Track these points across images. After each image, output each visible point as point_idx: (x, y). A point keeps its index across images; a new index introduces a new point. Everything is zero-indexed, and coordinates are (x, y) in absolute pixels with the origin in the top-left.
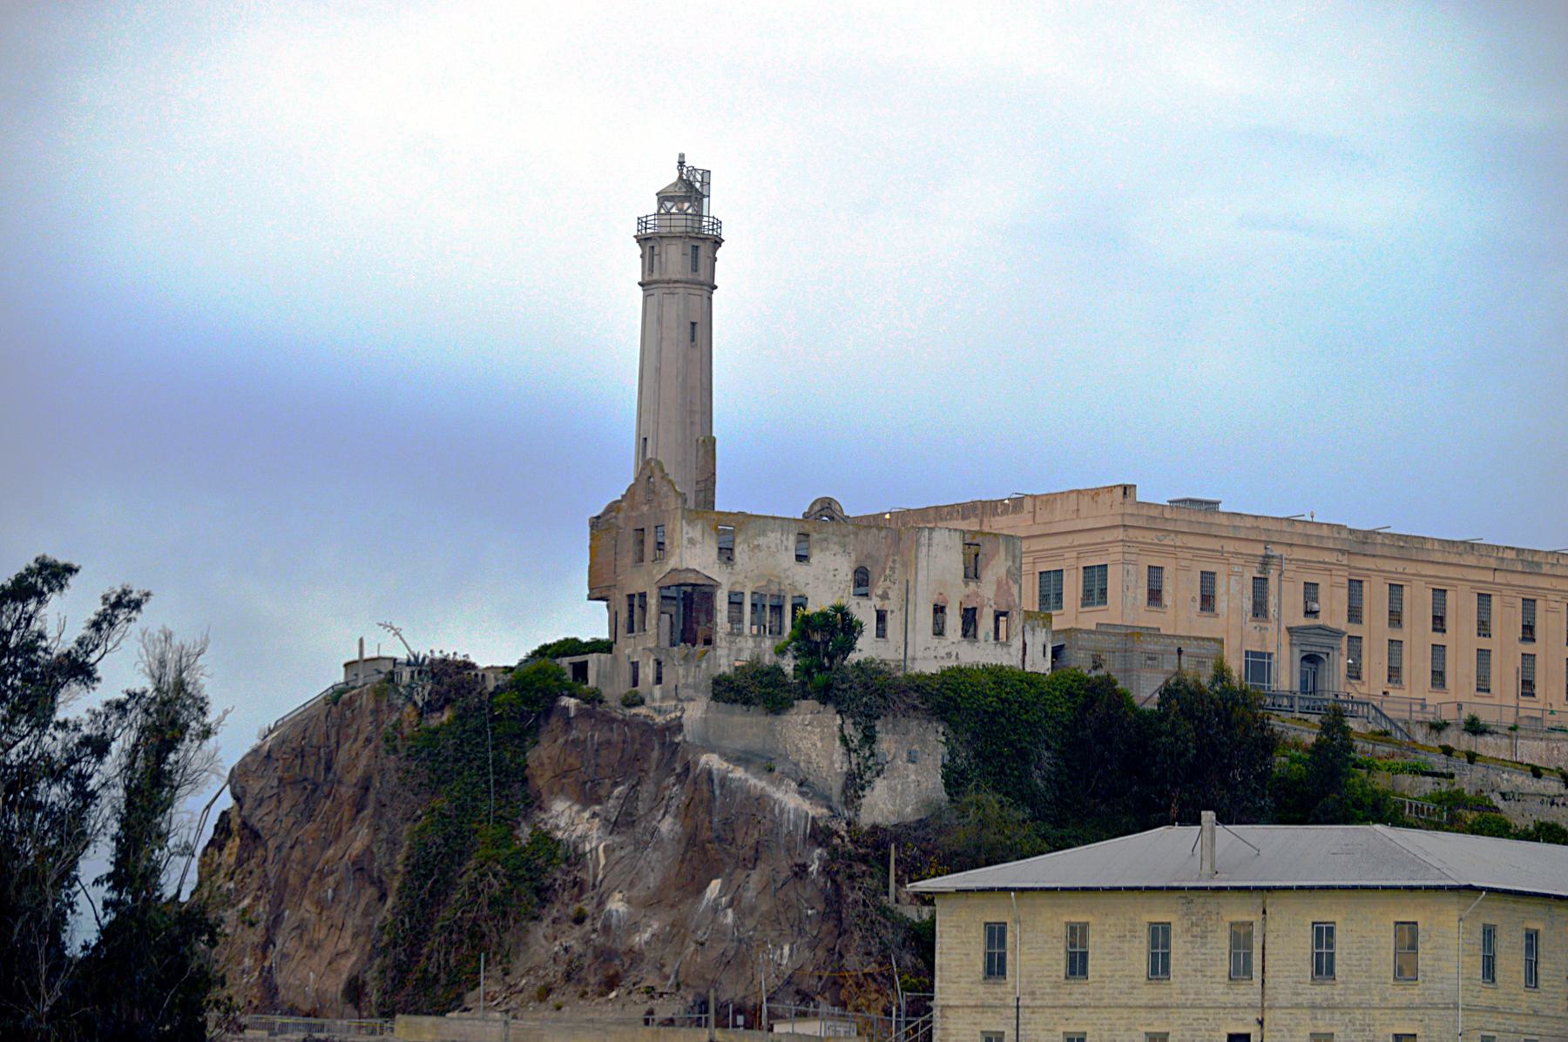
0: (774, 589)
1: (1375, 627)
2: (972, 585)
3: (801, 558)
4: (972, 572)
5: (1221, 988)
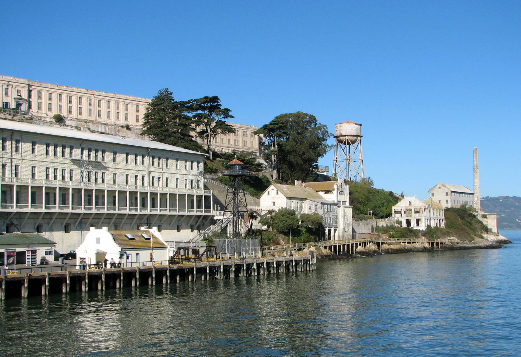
1: (34, 100)
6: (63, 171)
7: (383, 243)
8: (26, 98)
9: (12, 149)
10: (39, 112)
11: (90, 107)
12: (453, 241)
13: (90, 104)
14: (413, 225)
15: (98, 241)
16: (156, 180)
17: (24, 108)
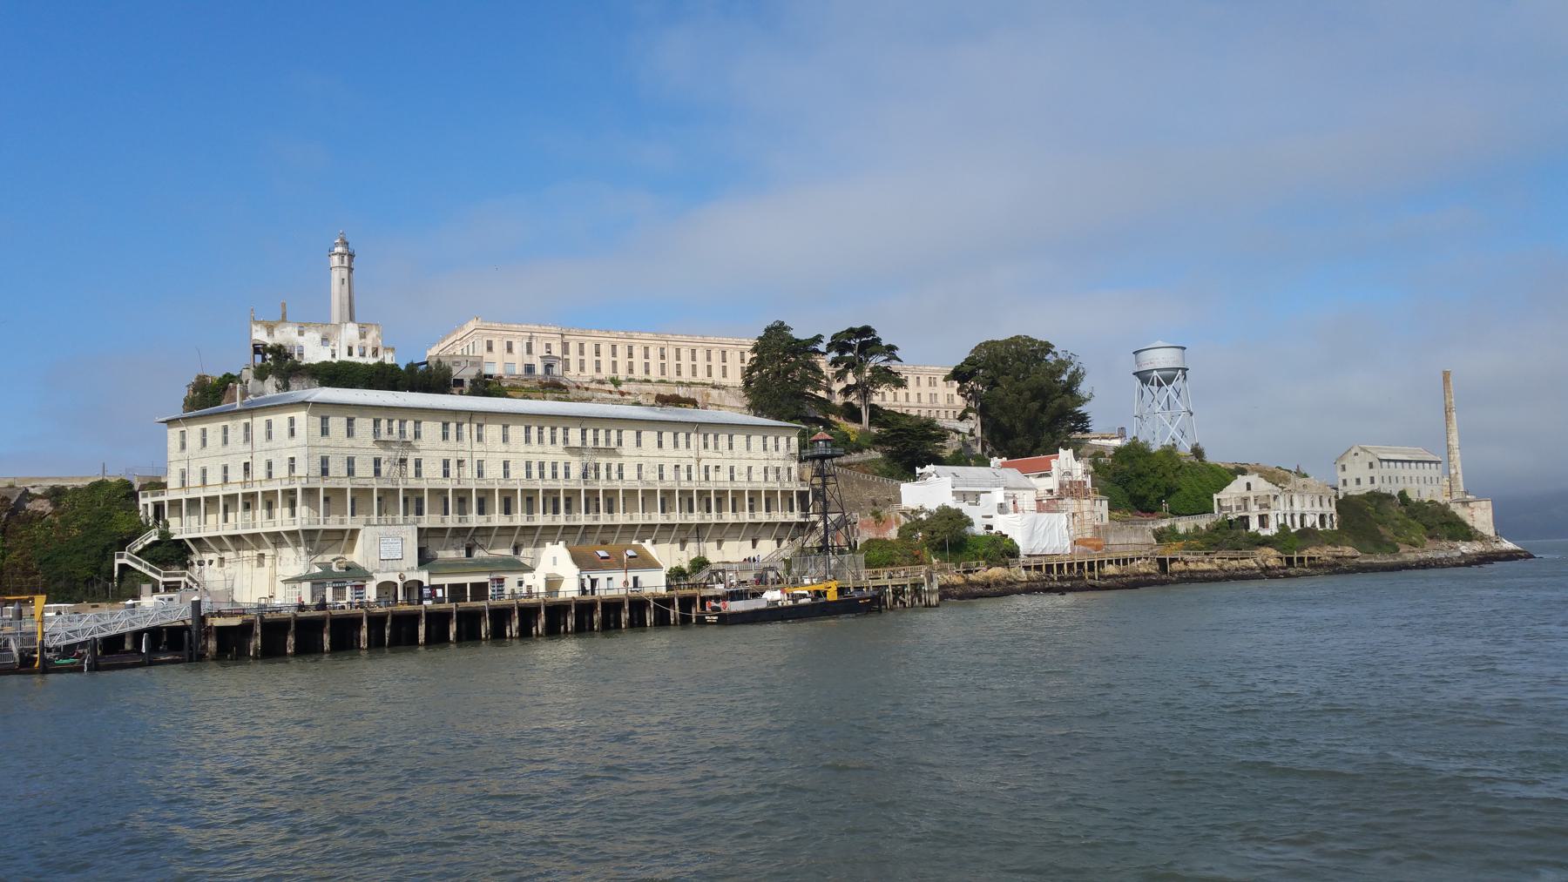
0: (290, 344)
1: (573, 356)
2: (363, 340)
3: (301, 333)
4: (363, 336)
5: (241, 447)
6: (554, 466)
7: (1172, 560)
9: (471, 437)
10: (582, 374)
11: (663, 361)
13: (663, 357)
14: (1254, 525)
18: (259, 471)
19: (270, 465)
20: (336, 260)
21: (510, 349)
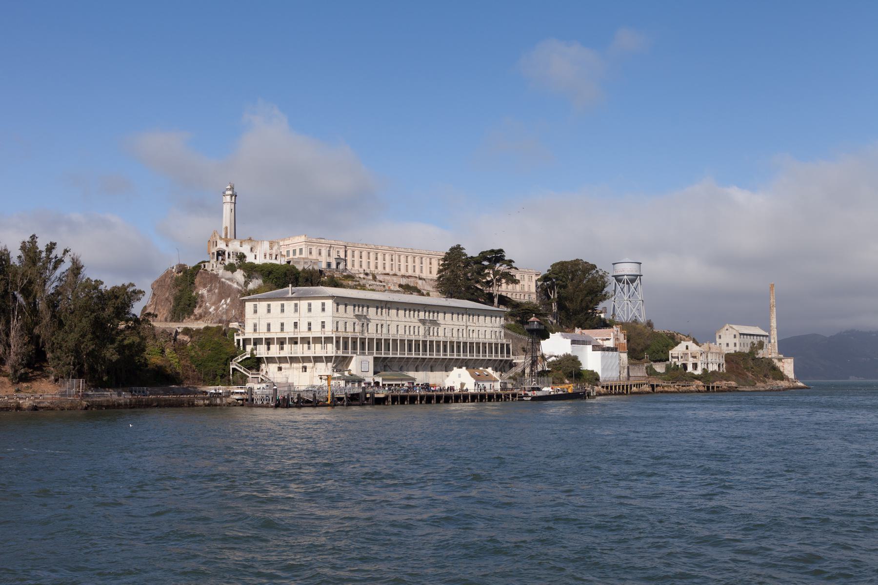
1: (349, 258)
4: (271, 248)
7: (657, 386)
8: (344, 258)
11: (392, 263)
12: (730, 385)
13: (392, 260)
14: (690, 369)
15: (459, 376)
16: (471, 331)
17: (341, 266)
18: (303, 327)
19: (310, 324)
20: (228, 198)
21: (320, 254)
